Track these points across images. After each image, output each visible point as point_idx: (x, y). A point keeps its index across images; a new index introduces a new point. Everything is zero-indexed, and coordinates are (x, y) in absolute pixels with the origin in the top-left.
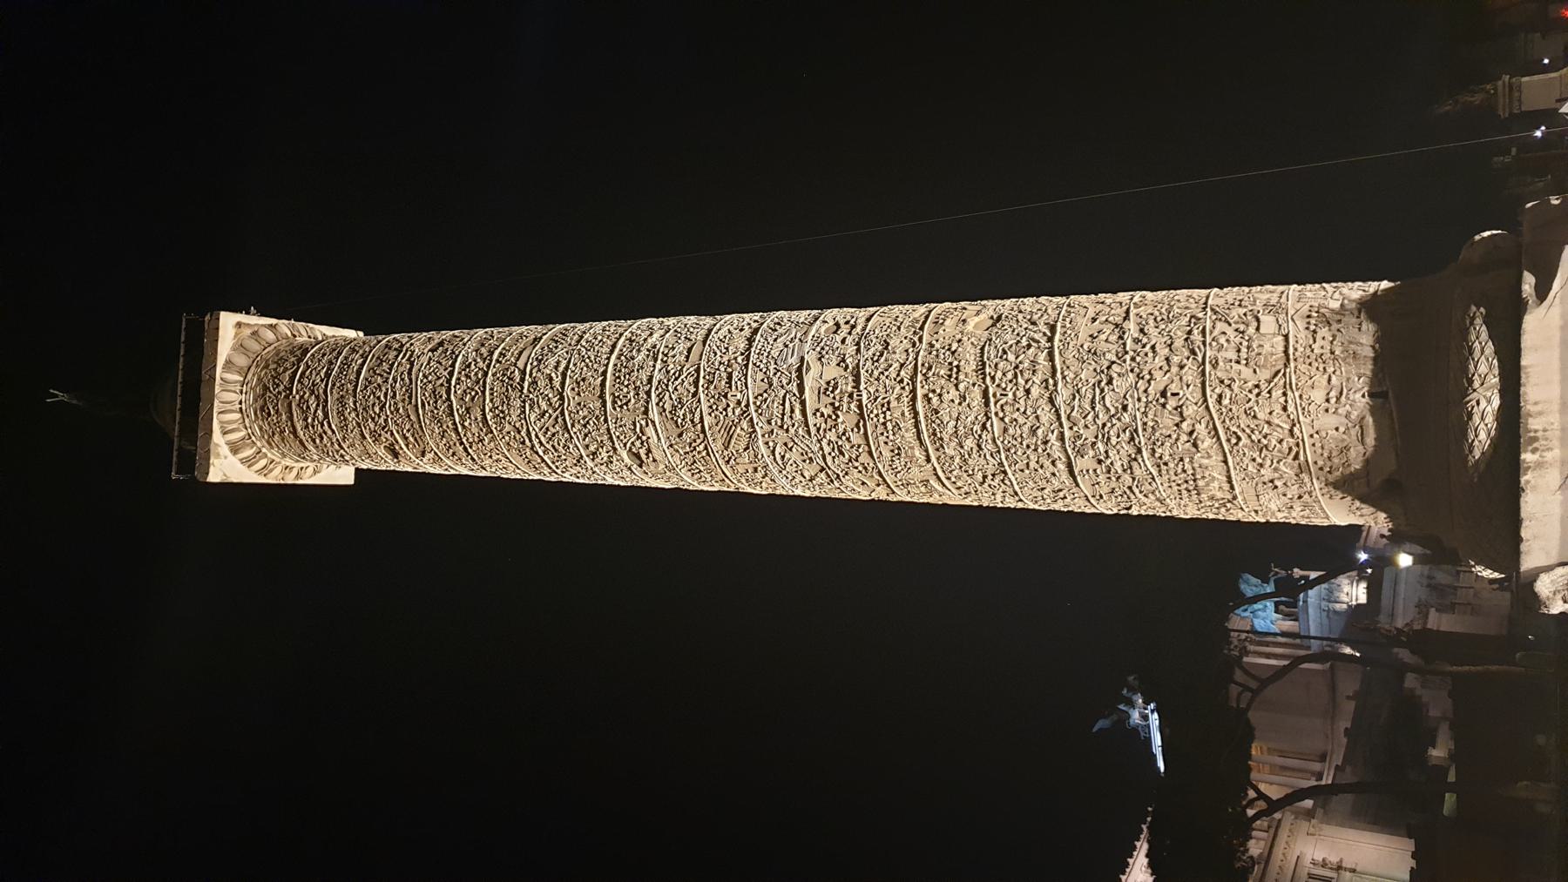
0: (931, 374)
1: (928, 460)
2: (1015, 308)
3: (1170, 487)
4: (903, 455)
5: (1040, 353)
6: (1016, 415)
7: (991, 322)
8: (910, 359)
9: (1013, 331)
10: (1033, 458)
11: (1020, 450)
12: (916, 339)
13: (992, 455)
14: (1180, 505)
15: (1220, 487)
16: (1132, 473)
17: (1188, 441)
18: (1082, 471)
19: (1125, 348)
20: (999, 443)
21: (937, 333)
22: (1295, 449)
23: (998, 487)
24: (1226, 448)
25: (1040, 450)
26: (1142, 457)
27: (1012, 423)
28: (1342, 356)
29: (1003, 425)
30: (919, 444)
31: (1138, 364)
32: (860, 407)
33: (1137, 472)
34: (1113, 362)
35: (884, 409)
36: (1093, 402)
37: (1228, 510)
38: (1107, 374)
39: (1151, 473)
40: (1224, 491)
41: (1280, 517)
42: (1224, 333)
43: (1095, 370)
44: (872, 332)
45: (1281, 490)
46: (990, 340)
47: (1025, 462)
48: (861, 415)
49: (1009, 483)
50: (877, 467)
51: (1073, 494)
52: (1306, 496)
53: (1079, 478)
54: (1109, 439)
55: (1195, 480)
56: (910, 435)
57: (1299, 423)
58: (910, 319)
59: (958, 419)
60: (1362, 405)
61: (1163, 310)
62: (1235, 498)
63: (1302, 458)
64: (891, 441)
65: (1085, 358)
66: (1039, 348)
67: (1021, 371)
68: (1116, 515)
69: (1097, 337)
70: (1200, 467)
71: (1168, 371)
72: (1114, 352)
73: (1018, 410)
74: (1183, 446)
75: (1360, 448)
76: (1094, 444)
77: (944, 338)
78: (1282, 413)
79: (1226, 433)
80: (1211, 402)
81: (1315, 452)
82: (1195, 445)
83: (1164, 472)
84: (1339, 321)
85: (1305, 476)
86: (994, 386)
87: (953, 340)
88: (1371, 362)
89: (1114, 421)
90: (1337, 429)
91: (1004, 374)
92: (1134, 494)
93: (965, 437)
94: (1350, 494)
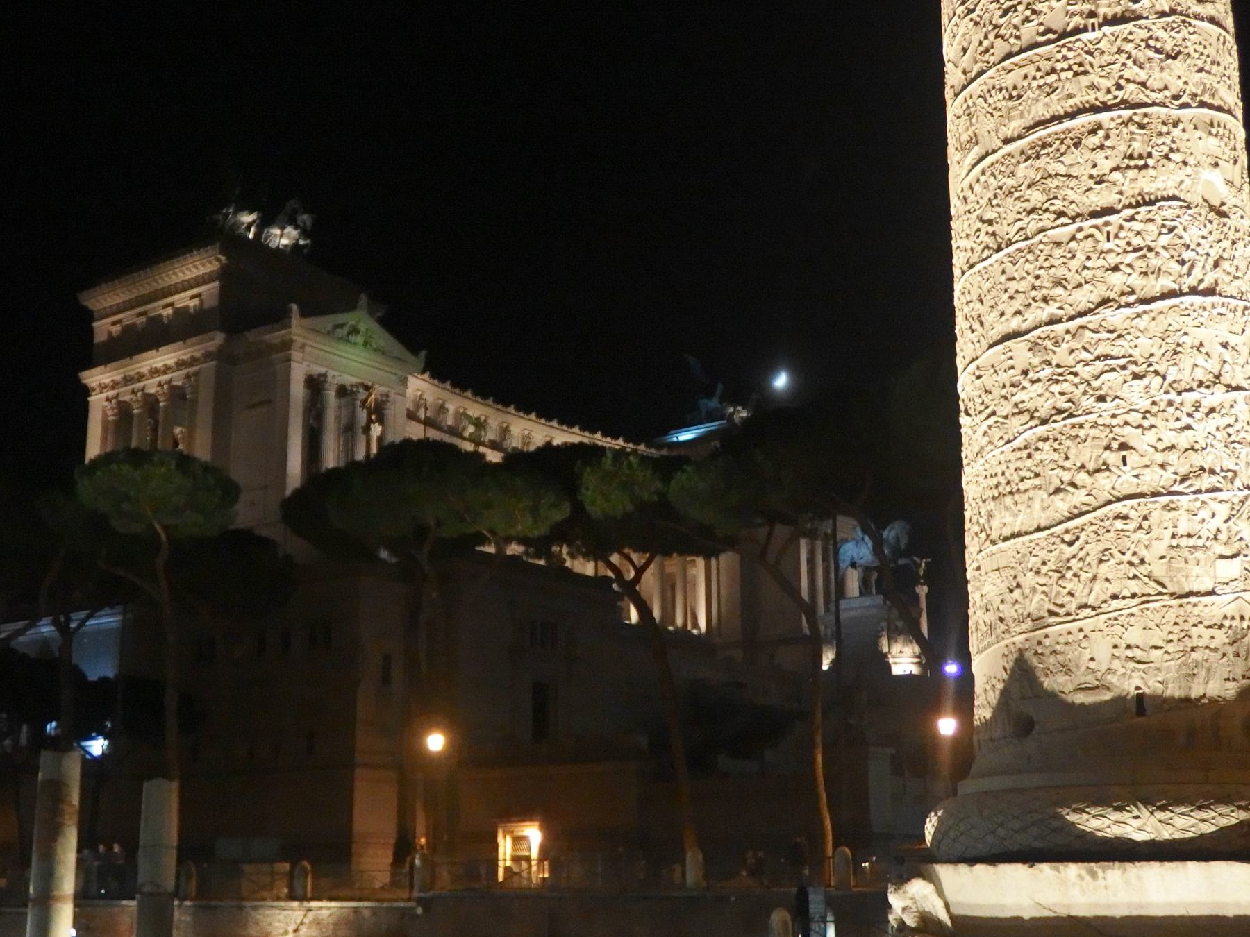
0: (1133, 128)
1: (1007, 141)
2: (1238, 235)
3: (1000, 463)
4: (1011, 104)
5: (1172, 278)
6: (1081, 257)
7: (1216, 203)
8: (1154, 95)
9: (1204, 237)
10: (1023, 286)
11: (1032, 267)
12: (1186, 99)
13: (1022, 229)
14: (978, 476)
15: (1005, 524)
16: (1014, 414)
17: (1062, 482)
18: (1010, 351)
19: (1186, 390)
20: (1040, 236)
21: (1196, 128)
22: (1062, 611)
23: (978, 241)
24: (1058, 529)
25: (1034, 293)
26: (1036, 426)
27: (1069, 252)
28: (1190, 661)
29: (1065, 240)
30: (1027, 125)
31: (1164, 411)
32: (1077, 31)
33: (1016, 423)
34: (1164, 378)
35: (1075, 68)
36: (1107, 357)
37: (977, 534)
38: (1147, 372)
39: (1015, 438)
40: (1001, 528)
41: (974, 597)
42: (1214, 515)
43: (1152, 355)
44: (1191, 30)
45: (1008, 597)
46: (1189, 207)
47: (1016, 275)
48: (1064, 35)
49: (984, 256)
50: (990, 68)
51: (979, 342)
52: (1003, 627)
53: (1000, 347)
54: (1057, 382)
55: (1011, 493)
56: (1041, 111)
57: (1097, 615)
58: (1215, 84)
59: (1069, 176)
60: (1127, 688)
61: (1243, 434)
62: (993, 542)
63: (1052, 620)
64: (1030, 84)
65: (1168, 340)
66: (1180, 276)
67: (1145, 256)
68: (958, 397)
69: (1200, 351)
70: (1030, 499)
71: (1156, 449)
72: (1179, 377)
73: (1089, 258)
74: (1055, 477)
75: (1071, 687)
76: (1049, 363)
77: (1188, 140)
78: (1109, 593)
79: (1077, 528)
80: (1118, 507)
81: (1061, 635)
82: (1058, 491)
83: (1018, 454)
84: (1237, 655)
85: (1028, 625)
86: (1121, 221)
87: (1186, 153)
88: (1183, 695)
89: (1082, 387)
90: (1092, 659)
91: (1138, 233)
92: (987, 418)
93: (1044, 190)
94: (1011, 677)
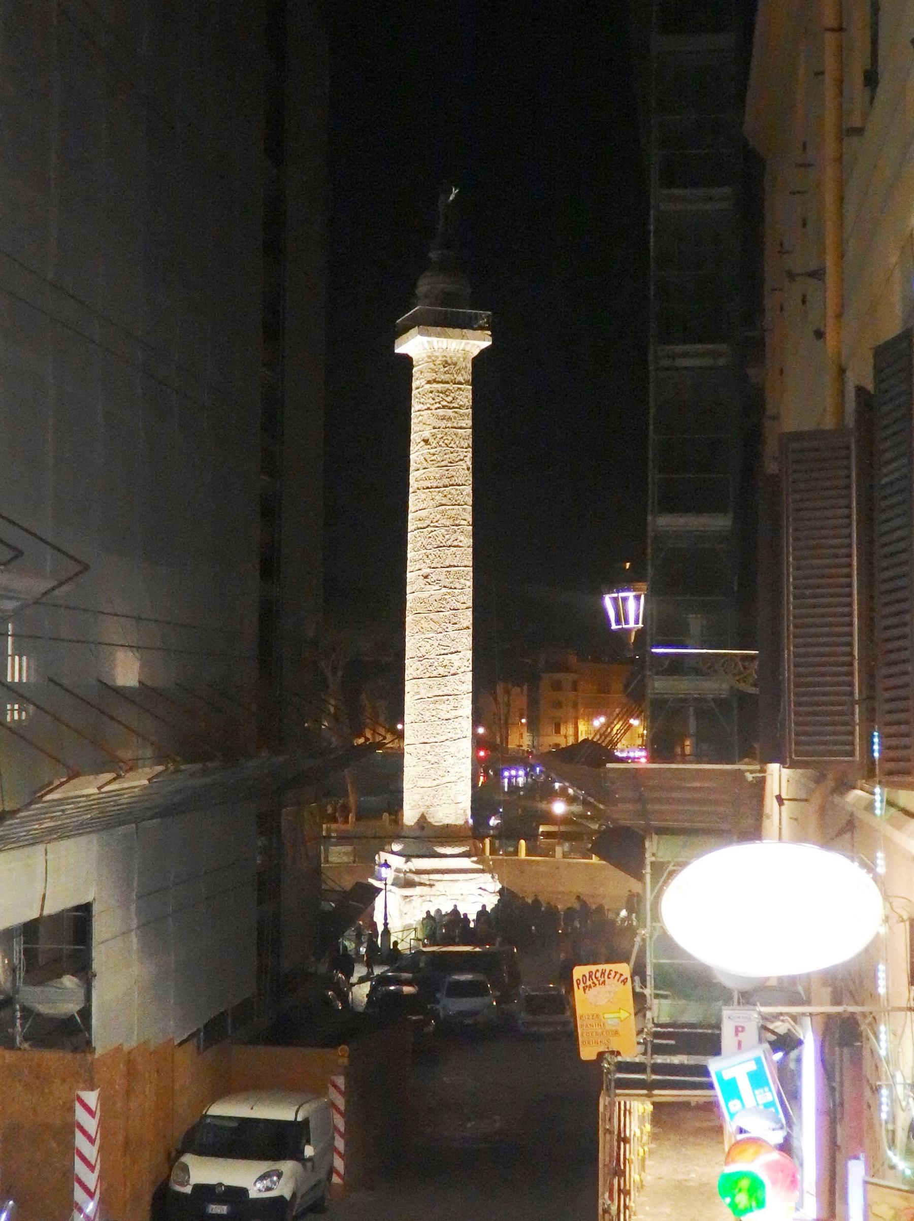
80: (447, 785)
